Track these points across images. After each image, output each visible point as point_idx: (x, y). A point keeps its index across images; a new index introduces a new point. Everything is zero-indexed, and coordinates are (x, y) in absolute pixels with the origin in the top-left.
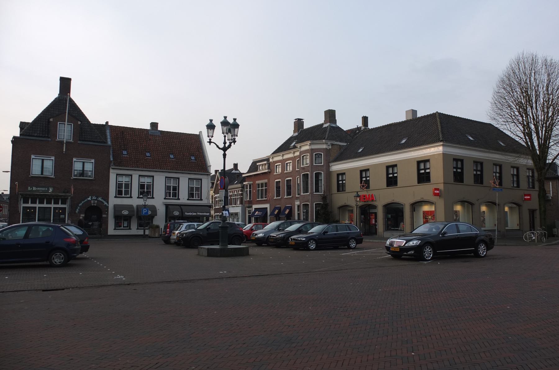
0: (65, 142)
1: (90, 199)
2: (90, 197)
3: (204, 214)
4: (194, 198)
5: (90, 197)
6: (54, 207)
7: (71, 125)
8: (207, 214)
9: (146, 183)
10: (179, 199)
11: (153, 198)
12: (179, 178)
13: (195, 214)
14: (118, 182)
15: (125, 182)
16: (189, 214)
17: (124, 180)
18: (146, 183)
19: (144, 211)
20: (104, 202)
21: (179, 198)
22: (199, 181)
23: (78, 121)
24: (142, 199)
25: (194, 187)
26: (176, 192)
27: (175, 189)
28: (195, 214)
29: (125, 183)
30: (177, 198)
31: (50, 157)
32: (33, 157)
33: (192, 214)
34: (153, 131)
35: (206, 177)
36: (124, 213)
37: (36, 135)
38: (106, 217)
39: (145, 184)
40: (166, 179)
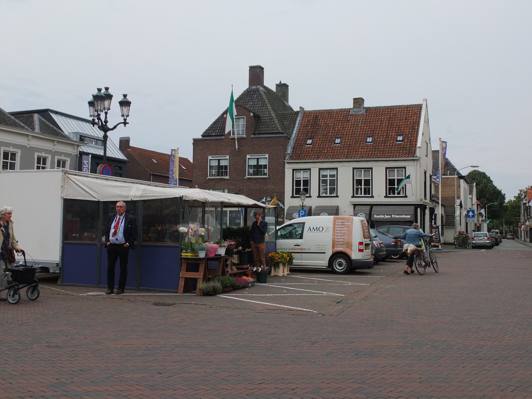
0: (236, 138)
1: (265, 201)
2: (265, 198)
3: (402, 216)
4: (395, 194)
5: (265, 198)
6: (229, 211)
7: (244, 118)
8: (406, 217)
9: (328, 178)
10: (372, 197)
11: (337, 196)
12: (372, 168)
13: (389, 217)
14: (295, 179)
15: (303, 178)
16: (379, 217)
17: (301, 176)
18: (328, 176)
19: (301, 213)
20: (280, 203)
21: (338, 195)
22: (403, 170)
23: (251, 112)
24: (299, 199)
25: (361, 180)
26: (370, 188)
27: (367, 182)
28: (389, 217)
29: (303, 180)
30: (370, 195)
31: (226, 157)
32: (210, 158)
33: (383, 216)
34: (356, 110)
35: (411, 163)
36: (295, 216)
37: (214, 134)
38: (282, 221)
39: (301, 180)
40: (355, 170)
